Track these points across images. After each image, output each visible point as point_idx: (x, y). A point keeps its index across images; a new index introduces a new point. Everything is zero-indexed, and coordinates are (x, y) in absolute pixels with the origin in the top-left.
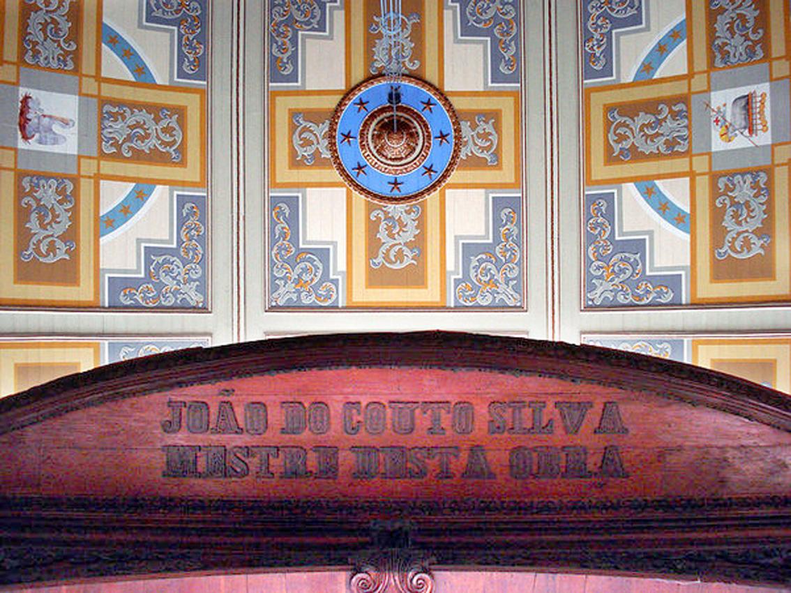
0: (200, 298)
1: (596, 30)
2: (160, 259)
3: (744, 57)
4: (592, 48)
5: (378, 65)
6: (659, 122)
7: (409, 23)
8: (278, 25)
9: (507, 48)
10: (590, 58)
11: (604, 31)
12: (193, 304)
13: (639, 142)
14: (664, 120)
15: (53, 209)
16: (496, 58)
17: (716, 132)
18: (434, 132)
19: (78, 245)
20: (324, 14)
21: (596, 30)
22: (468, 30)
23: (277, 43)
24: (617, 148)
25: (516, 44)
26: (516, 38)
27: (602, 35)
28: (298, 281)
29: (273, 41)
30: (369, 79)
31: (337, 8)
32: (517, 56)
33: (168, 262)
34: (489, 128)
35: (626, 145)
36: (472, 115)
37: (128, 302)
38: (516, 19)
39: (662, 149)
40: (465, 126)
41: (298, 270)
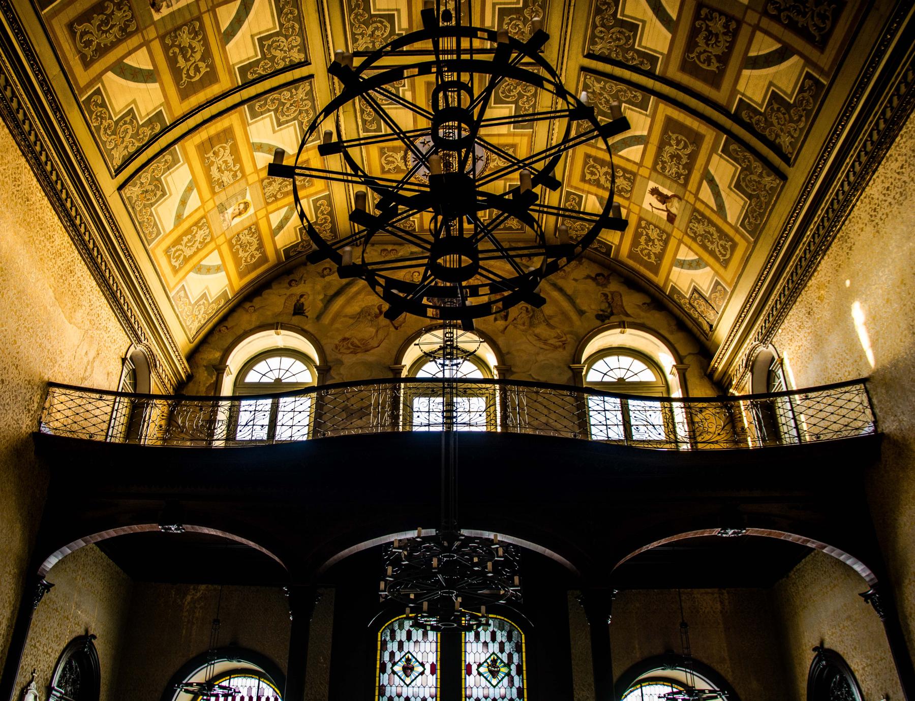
0: (302, 56)
2: (270, 42)
12: (297, 61)
15: (190, 46)
19: (213, 59)
24: (588, 177)
28: (372, 35)
33: (276, 41)
37: (255, 76)
41: (371, 29)
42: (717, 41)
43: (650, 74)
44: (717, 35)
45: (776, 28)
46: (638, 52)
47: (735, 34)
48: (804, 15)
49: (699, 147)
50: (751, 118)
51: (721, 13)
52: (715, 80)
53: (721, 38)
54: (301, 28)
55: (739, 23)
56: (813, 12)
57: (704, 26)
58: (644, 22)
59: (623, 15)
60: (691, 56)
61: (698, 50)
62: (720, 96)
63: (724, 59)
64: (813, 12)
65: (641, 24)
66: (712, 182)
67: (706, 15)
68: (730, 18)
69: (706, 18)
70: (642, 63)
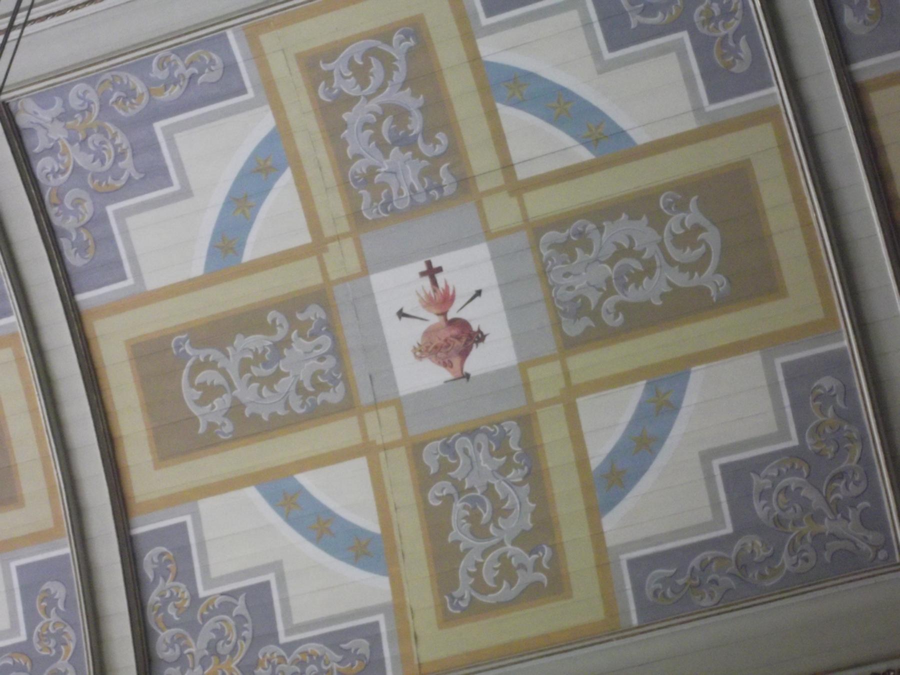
45: (403, 494)
47: (319, 414)
48: (479, 531)
52: (178, 438)
55: (348, 406)
56: (501, 543)
58: (186, 192)
60: (187, 348)
64: (501, 543)
65: (176, 187)
67: (309, 321)
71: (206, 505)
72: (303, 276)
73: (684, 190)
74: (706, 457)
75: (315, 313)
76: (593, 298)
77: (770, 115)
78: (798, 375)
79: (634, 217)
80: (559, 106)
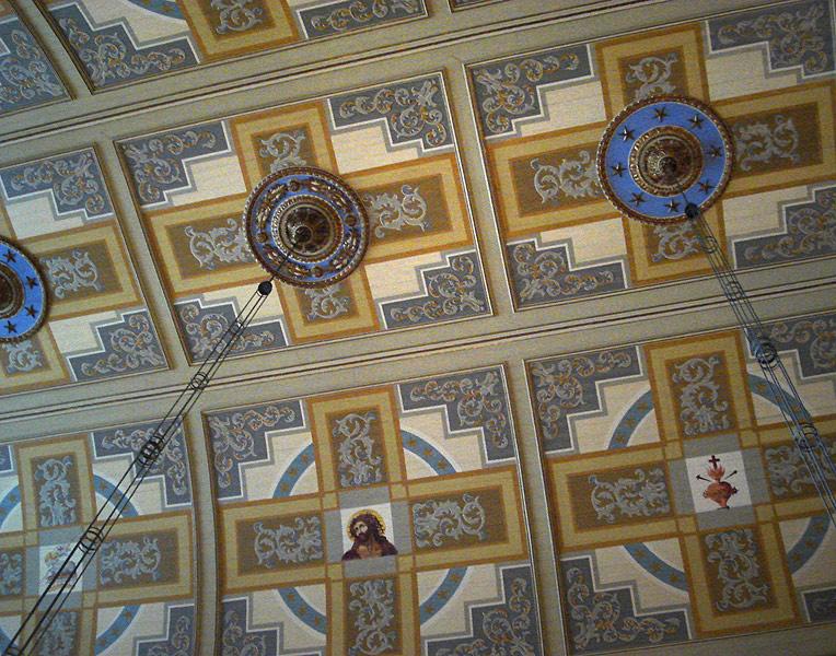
1: (134, 438)
3: (104, 568)
4: (119, 436)
5: (48, 263)
6: (62, 500)
7: (92, 284)
8: (52, 168)
9: (103, 366)
10: (111, 435)
11: (133, 444)
13: (48, 486)
14: (64, 505)
16: (92, 359)
17: (52, 549)
18: (13, 320)
20: (74, 208)
21: (134, 438)
22: (105, 333)
23: (36, 171)
24: (43, 467)
25: (107, 374)
26: (113, 372)
27: (129, 444)
29: (36, 167)
30: (33, 260)
31: (84, 219)
32: (98, 375)
34: (34, 363)
35: (46, 475)
36: (37, 346)
38: (129, 370)
39: (43, 506)
40: (27, 344)
42: (291, 548)
43: (216, 492)
44: (297, 546)
46: (235, 466)
47: (309, 563)
49: (160, 581)
50: (232, 621)
51: (322, 537)
52: (248, 565)
53: (297, 551)
54: (141, 76)
57: (300, 528)
59: (270, 437)
61: (270, 532)
62: (234, 580)
63: (278, 564)
64: (376, 630)
66: (128, 616)
68: (322, 548)
69: (309, 527)
70: (225, 479)
71: (256, 594)
72: (314, 505)
73: (473, 493)
74: (466, 604)
75: (314, 520)
76: (431, 532)
77: (512, 467)
78: (509, 577)
79: (452, 501)
80: (427, 452)
